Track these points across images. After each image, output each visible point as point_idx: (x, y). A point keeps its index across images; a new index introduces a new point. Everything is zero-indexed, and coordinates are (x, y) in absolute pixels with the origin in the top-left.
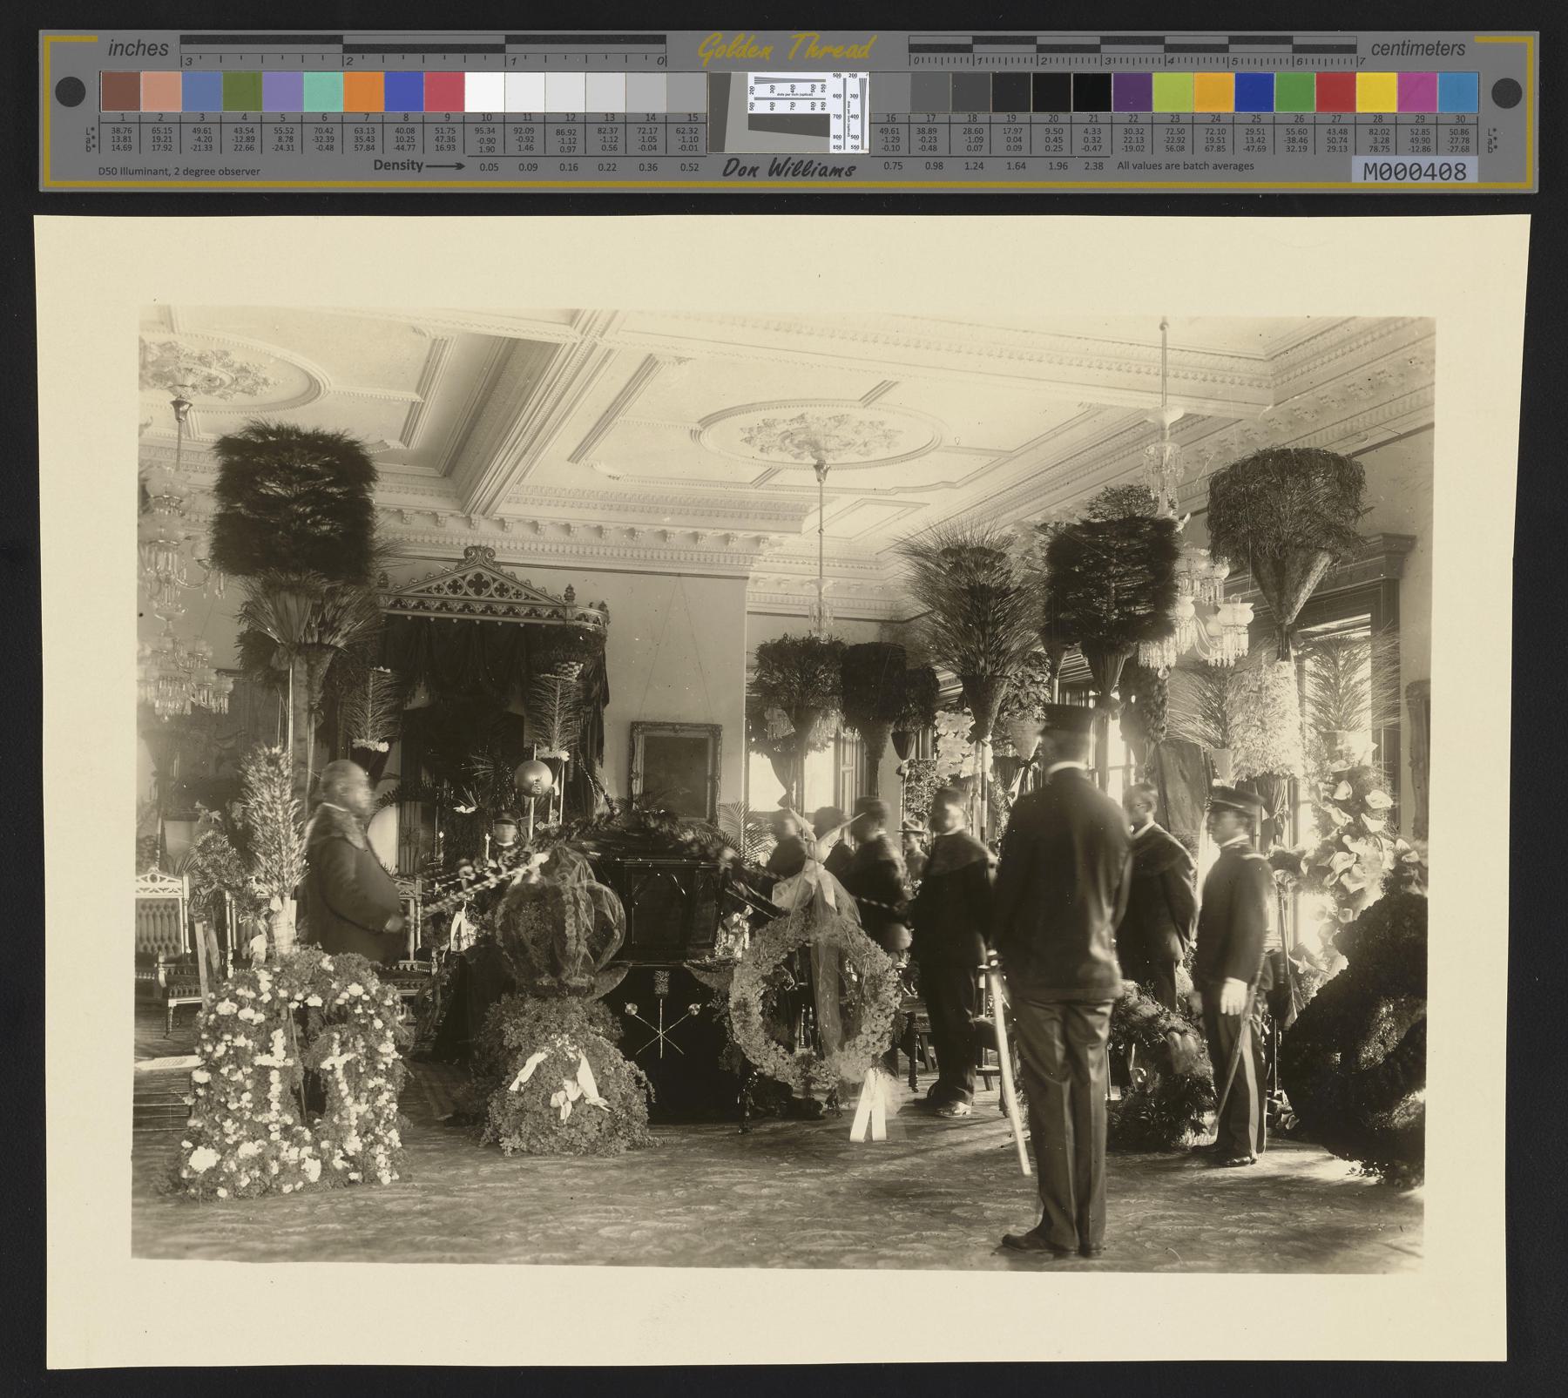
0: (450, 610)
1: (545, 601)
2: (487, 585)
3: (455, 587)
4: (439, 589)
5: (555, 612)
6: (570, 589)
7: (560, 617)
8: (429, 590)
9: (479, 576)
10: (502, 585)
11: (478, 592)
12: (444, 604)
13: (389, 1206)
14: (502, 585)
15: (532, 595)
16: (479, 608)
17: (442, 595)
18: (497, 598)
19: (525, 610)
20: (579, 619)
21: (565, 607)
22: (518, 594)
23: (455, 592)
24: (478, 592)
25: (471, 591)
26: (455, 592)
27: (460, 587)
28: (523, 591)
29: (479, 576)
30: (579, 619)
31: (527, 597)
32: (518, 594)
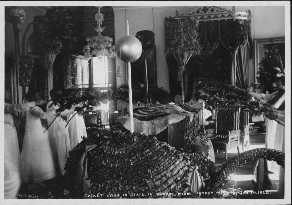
4: (193, 13)
5: (230, 15)
7: (231, 16)
8: (190, 14)
11: (205, 12)
13: (194, 171)
14: (212, 9)
15: (222, 10)
16: (206, 17)
17: (194, 15)
18: (211, 13)
19: (220, 16)
20: (238, 16)
21: (232, 13)
23: (198, 13)
24: (205, 12)
25: (203, 12)
26: (198, 13)
28: (219, 10)
30: (238, 16)
31: (220, 11)
32: (217, 11)
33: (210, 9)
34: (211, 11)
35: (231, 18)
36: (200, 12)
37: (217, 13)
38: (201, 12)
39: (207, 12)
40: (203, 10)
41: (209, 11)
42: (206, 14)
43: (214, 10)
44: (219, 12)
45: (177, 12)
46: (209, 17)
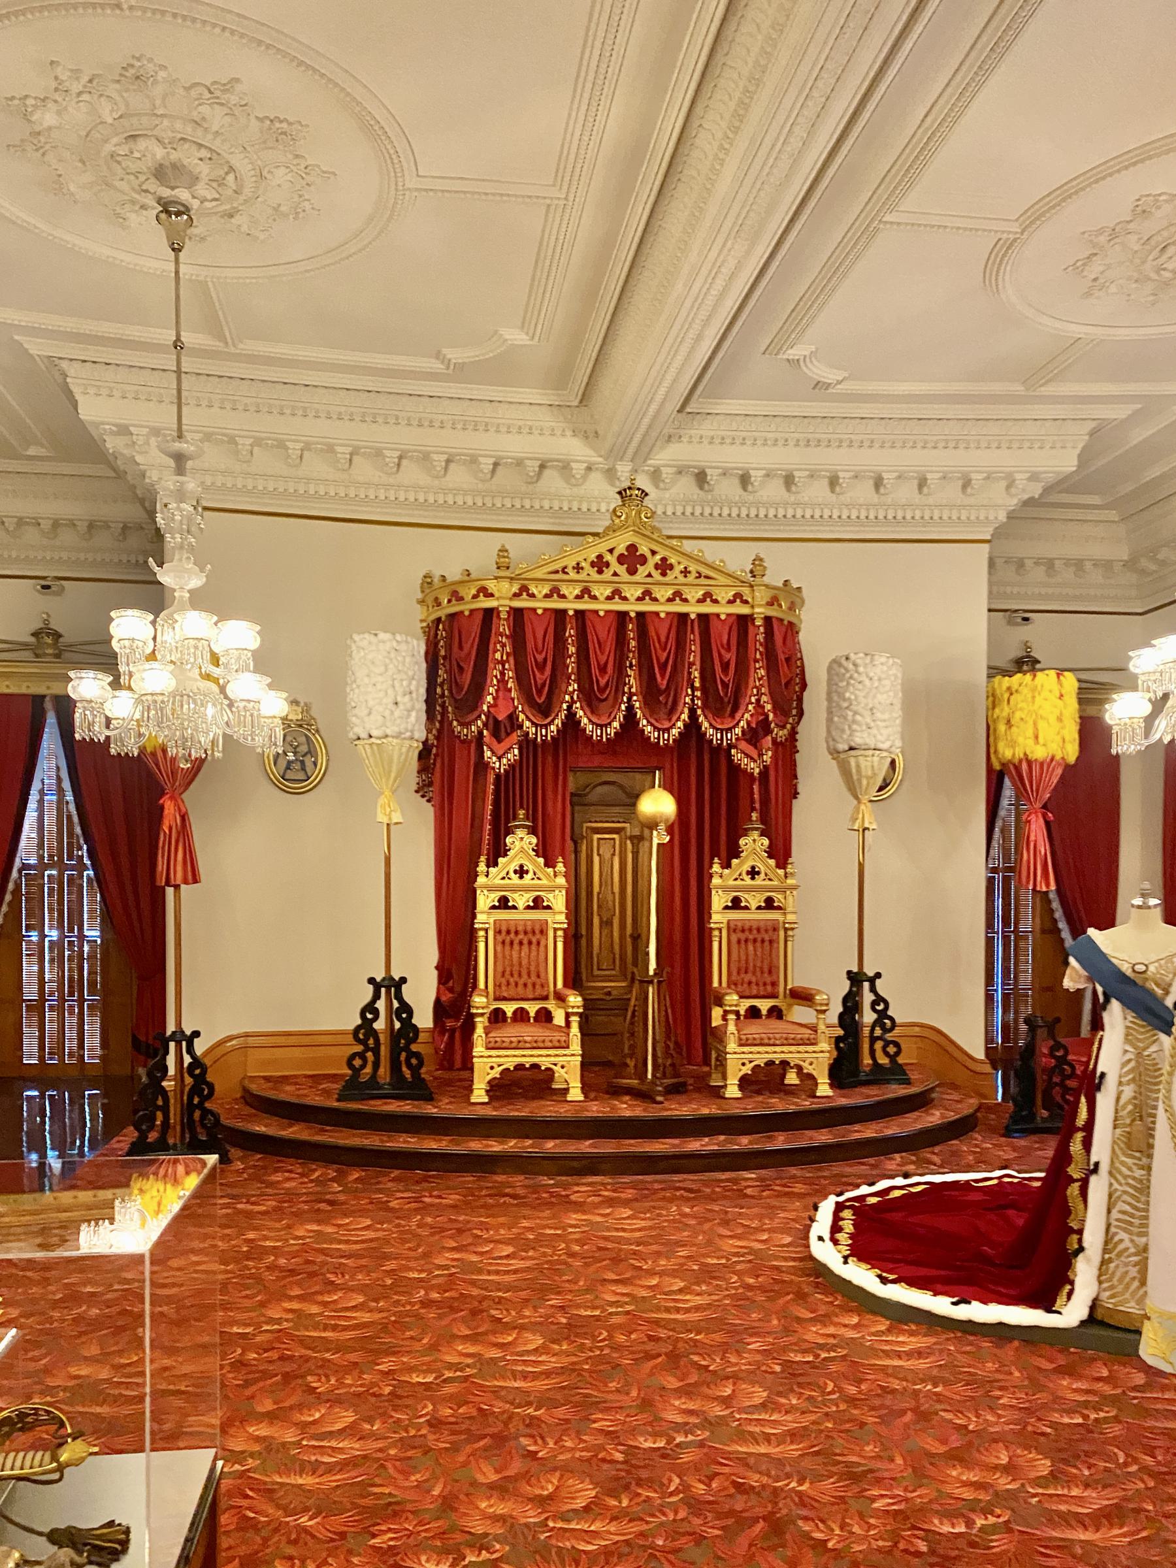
12: (586, 591)
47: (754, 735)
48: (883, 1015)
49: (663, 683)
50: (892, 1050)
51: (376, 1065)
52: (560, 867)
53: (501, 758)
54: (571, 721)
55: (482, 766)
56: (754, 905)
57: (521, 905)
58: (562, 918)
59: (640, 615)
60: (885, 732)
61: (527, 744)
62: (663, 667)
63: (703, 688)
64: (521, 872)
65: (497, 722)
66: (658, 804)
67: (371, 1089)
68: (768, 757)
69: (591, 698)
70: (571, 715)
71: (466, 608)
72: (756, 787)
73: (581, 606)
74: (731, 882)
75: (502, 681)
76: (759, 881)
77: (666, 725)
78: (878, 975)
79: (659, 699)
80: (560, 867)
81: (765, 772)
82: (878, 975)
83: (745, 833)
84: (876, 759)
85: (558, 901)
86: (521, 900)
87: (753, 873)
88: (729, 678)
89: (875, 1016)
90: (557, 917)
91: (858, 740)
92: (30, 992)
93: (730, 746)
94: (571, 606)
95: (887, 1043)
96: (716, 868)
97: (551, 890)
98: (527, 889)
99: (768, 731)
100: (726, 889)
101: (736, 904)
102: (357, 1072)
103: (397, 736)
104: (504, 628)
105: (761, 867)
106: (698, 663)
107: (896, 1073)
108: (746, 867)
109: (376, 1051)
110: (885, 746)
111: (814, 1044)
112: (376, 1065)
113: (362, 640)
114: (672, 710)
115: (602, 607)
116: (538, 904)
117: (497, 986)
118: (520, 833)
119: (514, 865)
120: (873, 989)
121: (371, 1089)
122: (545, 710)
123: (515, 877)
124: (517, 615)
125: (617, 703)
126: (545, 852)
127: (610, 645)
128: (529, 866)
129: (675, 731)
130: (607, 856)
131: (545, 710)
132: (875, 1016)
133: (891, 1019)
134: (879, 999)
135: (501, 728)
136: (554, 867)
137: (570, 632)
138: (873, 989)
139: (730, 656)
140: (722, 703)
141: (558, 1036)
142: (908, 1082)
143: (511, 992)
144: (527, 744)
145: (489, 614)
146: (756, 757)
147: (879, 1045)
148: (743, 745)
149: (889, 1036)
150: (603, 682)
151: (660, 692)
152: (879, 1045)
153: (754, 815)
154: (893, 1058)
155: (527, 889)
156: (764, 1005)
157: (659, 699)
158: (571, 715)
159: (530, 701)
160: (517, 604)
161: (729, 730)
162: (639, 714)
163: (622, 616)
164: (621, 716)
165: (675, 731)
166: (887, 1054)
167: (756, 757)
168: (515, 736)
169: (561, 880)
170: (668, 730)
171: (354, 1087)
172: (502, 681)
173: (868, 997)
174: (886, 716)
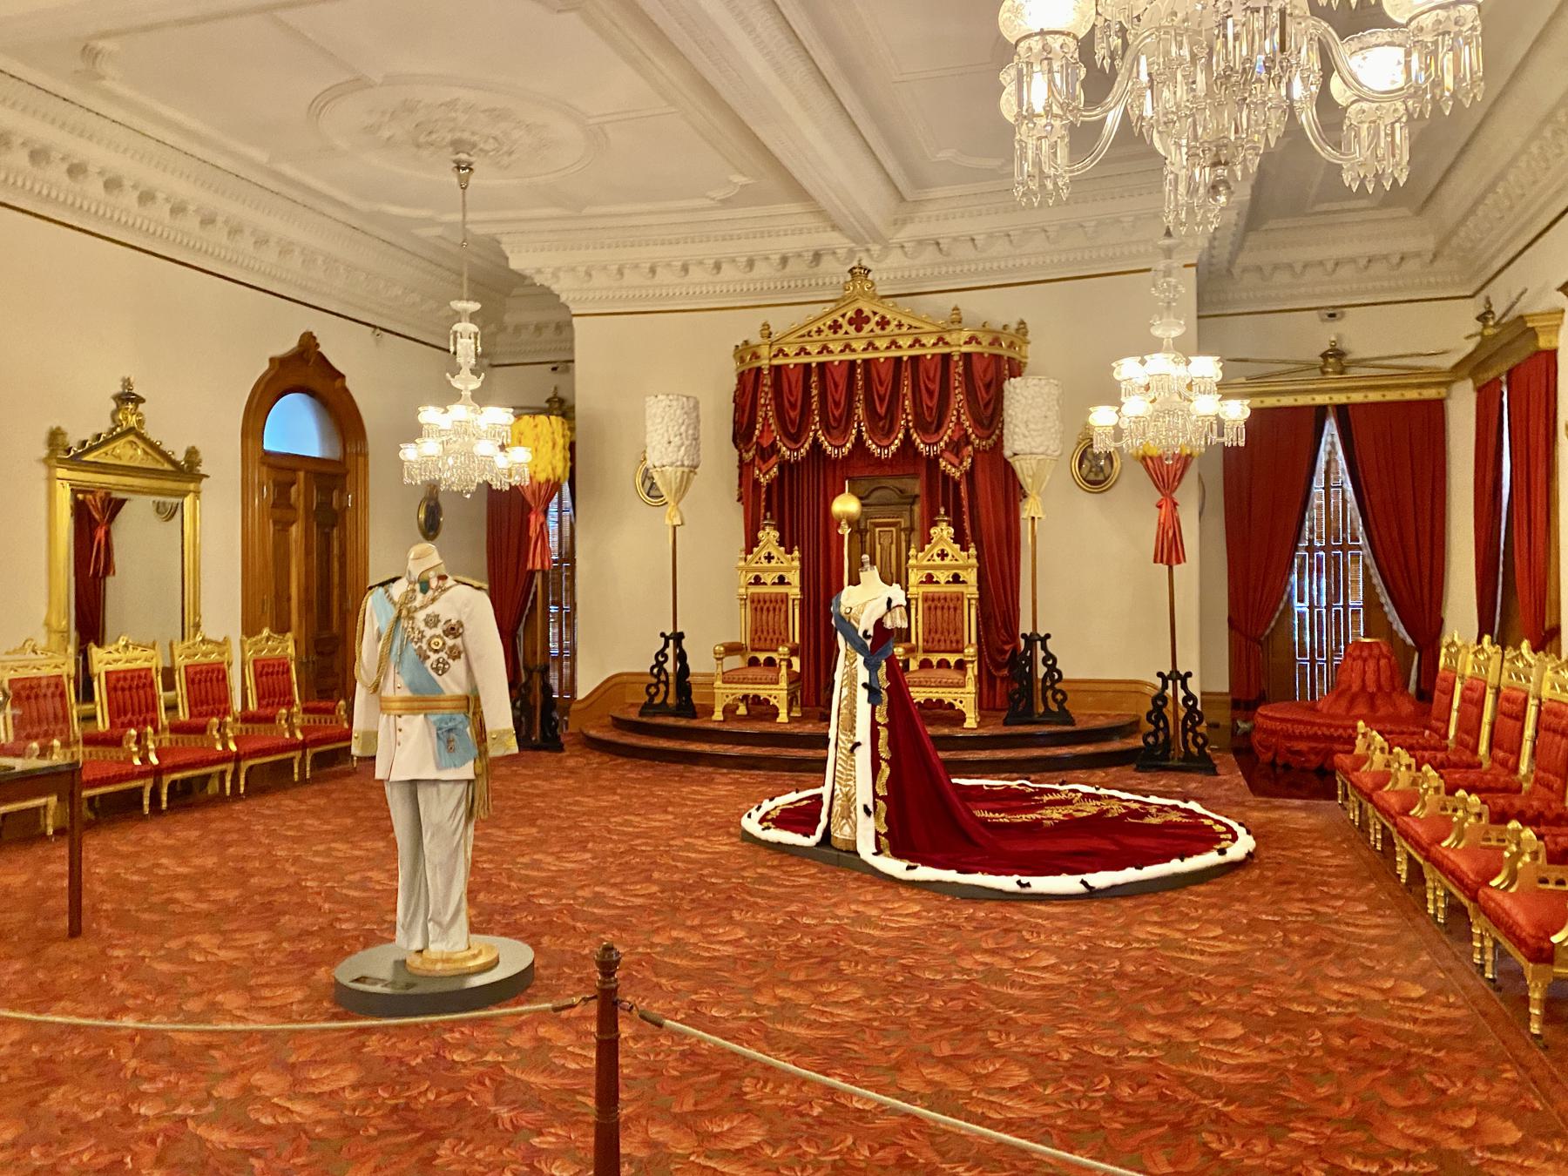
0: (831, 352)
1: (928, 328)
2: (867, 320)
3: (835, 327)
4: (819, 331)
5: (940, 339)
6: (956, 309)
7: (946, 344)
8: (809, 334)
9: (859, 312)
10: (883, 317)
11: (859, 329)
15: (914, 324)
22: (900, 325)
24: (859, 329)
27: (841, 327)
29: (859, 312)
31: (910, 327)
32: (900, 325)
33: (877, 318)
34: (878, 323)
35: (946, 350)
36: (841, 327)
37: (897, 331)
38: (846, 327)
39: (867, 328)
40: (851, 322)
41: (872, 325)
42: (862, 334)
43: (888, 323)
44: (904, 329)
45: (766, 326)
46: (871, 345)
47: (956, 447)
48: (1052, 668)
49: (882, 411)
50: (1059, 697)
51: (667, 693)
52: (796, 554)
53: (766, 475)
54: (816, 444)
55: (757, 483)
56: (943, 580)
57: (769, 581)
58: (797, 591)
59: (865, 361)
60: (1038, 440)
61: (784, 465)
62: (882, 400)
63: (916, 414)
64: (769, 558)
65: (763, 449)
66: (846, 505)
67: (663, 709)
68: (967, 463)
69: (828, 430)
70: (816, 439)
71: (746, 368)
72: (963, 488)
73: (822, 359)
74: (925, 562)
75: (766, 419)
76: (947, 561)
77: (885, 443)
78: (1048, 636)
79: (883, 424)
80: (796, 554)
81: (970, 475)
82: (1048, 636)
83: (935, 524)
84: (1034, 462)
85: (794, 578)
86: (768, 578)
87: (943, 555)
88: (934, 403)
89: (1045, 669)
90: (794, 591)
91: (1017, 448)
92: (555, 651)
93: (937, 457)
94: (814, 360)
95: (1056, 692)
96: (912, 552)
97: (789, 570)
98: (773, 570)
99: (969, 443)
100: (920, 568)
101: (930, 579)
102: (652, 697)
103: (672, 465)
104: (768, 381)
105: (948, 550)
106: (909, 395)
107: (1065, 717)
108: (937, 550)
109: (667, 683)
110: (1041, 450)
111: (964, 686)
112: (667, 693)
113: (651, 400)
114: (889, 432)
115: (836, 358)
116: (782, 581)
117: (753, 640)
118: (768, 529)
119: (764, 553)
120: (1044, 648)
121: (663, 709)
122: (795, 438)
123: (765, 563)
124: (777, 370)
125: (846, 431)
126: (786, 542)
127: (842, 386)
128: (774, 553)
129: (893, 448)
130: (886, 544)
131: (795, 438)
132: (1045, 669)
133: (1060, 673)
134: (1049, 656)
135: (767, 453)
136: (789, 551)
137: (814, 378)
138: (1044, 648)
139: (936, 387)
140: (930, 423)
141: (771, 675)
142: (1072, 723)
143: (762, 645)
144: (784, 465)
145: (759, 369)
146: (956, 462)
147: (1049, 693)
148: (947, 455)
149: (1057, 686)
150: (837, 413)
151: (881, 418)
152: (1049, 693)
153: (942, 511)
154: (1060, 704)
155: (773, 570)
156: (952, 659)
157: (883, 424)
158: (816, 439)
159: (786, 434)
160: (776, 362)
161: (936, 444)
162: (865, 436)
163: (853, 363)
164: (853, 438)
165: (893, 448)
166: (1055, 700)
167: (956, 462)
168: (774, 459)
169: (797, 563)
170: (887, 447)
171: (647, 708)
172: (766, 419)
173: (1041, 654)
174: (1040, 426)
